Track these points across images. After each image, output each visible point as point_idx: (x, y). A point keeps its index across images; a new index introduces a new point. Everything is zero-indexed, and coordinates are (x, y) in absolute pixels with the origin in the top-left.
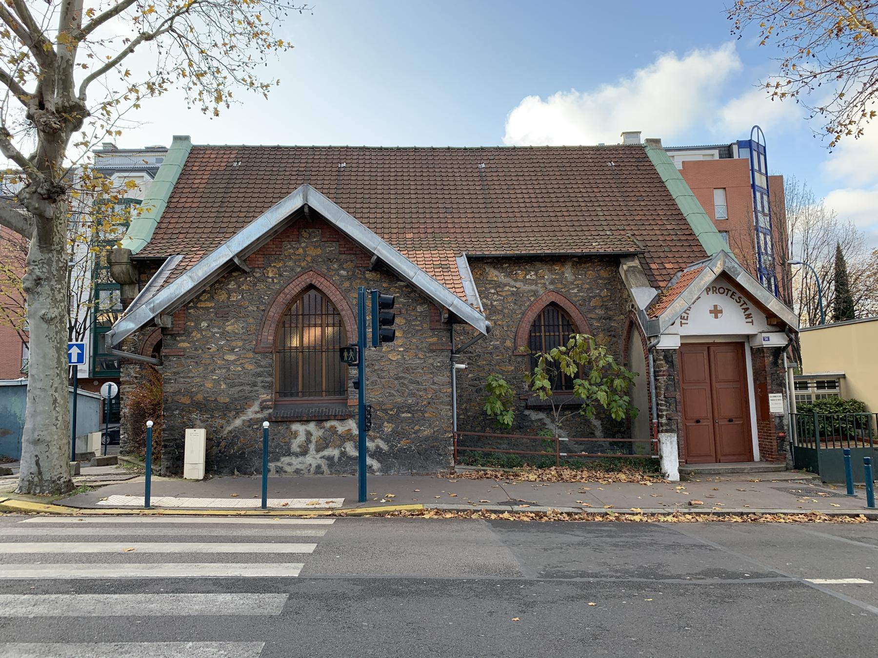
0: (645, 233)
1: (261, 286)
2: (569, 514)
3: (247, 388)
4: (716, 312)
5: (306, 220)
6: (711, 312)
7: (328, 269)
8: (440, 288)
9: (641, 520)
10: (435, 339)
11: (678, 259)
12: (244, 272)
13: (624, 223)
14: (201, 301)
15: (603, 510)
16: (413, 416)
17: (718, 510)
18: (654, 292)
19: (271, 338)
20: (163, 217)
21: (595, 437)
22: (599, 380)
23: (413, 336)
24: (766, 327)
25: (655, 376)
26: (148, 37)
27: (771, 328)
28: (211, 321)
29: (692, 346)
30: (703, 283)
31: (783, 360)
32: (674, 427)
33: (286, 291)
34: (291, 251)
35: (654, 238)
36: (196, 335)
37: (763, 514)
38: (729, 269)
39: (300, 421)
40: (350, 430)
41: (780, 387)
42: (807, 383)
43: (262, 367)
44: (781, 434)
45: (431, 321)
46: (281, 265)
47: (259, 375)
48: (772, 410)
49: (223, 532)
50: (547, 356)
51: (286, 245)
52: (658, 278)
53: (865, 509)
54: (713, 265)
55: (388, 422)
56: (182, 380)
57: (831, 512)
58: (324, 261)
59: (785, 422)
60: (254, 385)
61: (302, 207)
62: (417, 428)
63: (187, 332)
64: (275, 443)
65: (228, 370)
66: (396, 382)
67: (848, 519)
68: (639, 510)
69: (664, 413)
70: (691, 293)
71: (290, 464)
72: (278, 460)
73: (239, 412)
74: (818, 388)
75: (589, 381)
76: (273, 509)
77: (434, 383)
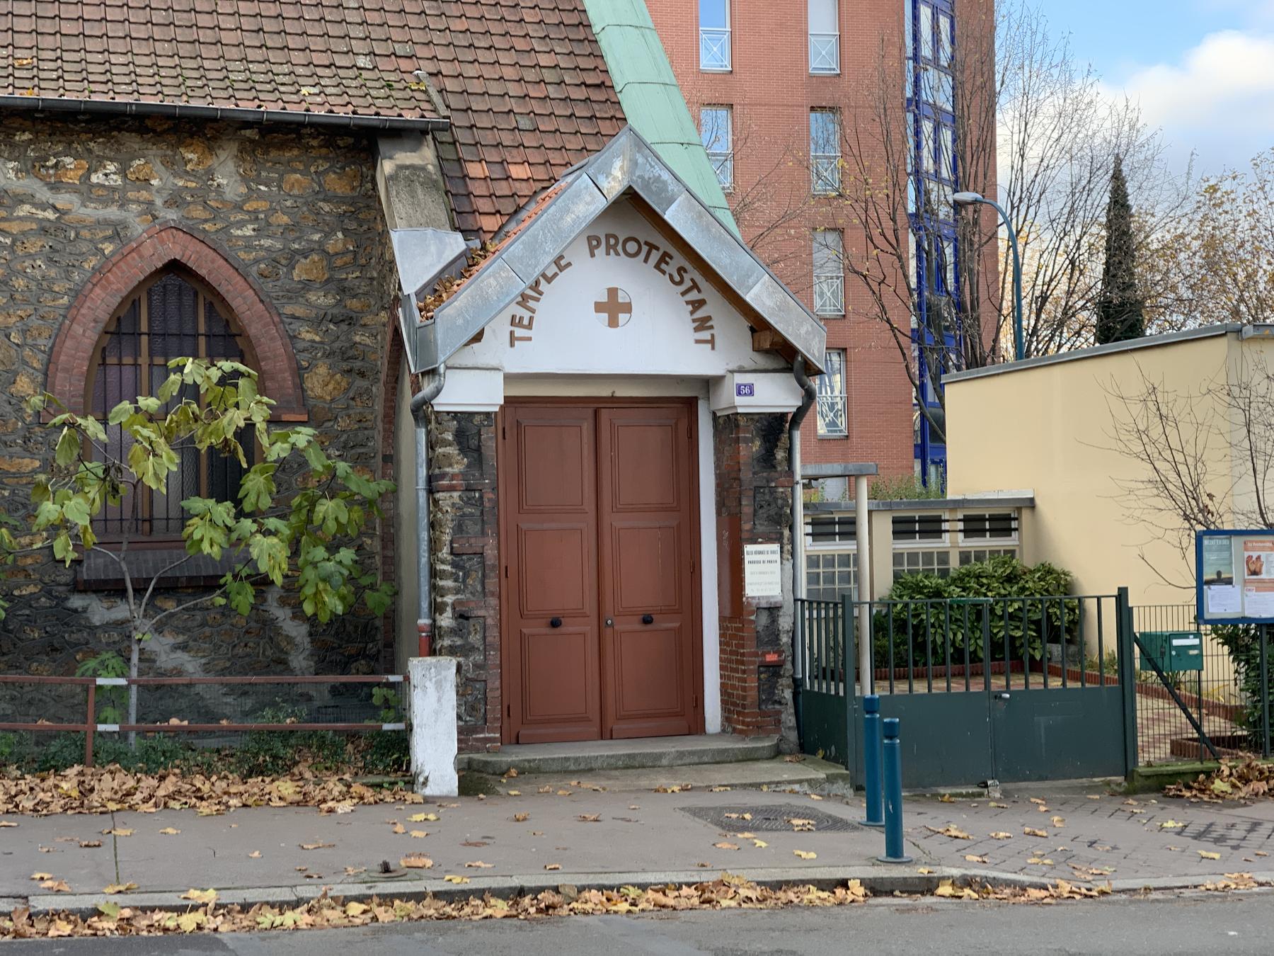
0: (470, 71)
4: (613, 308)
6: (599, 307)
9: (199, 927)
13: (417, 36)
15: (86, 902)
17: (458, 882)
18: (456, 244)
21: (289, 670)
22: (266, 502)
24: (748, 356)
25: (431, 491)
27: (761, 361)
29: (534, 410)
30: (569, 219)
31: (790, 451)
32: (475, 639)
35: (495, 88)
37: (581, 889)
38: (646, 184)
41: (777, 526)
42: (939, 520)
44: (771, 658)
50: (91, 426)
59: (785, 623)
67: (814, 894)
68: (211, 896)
69: (449, 599)
74: (968, 533)
75: (238, 503)
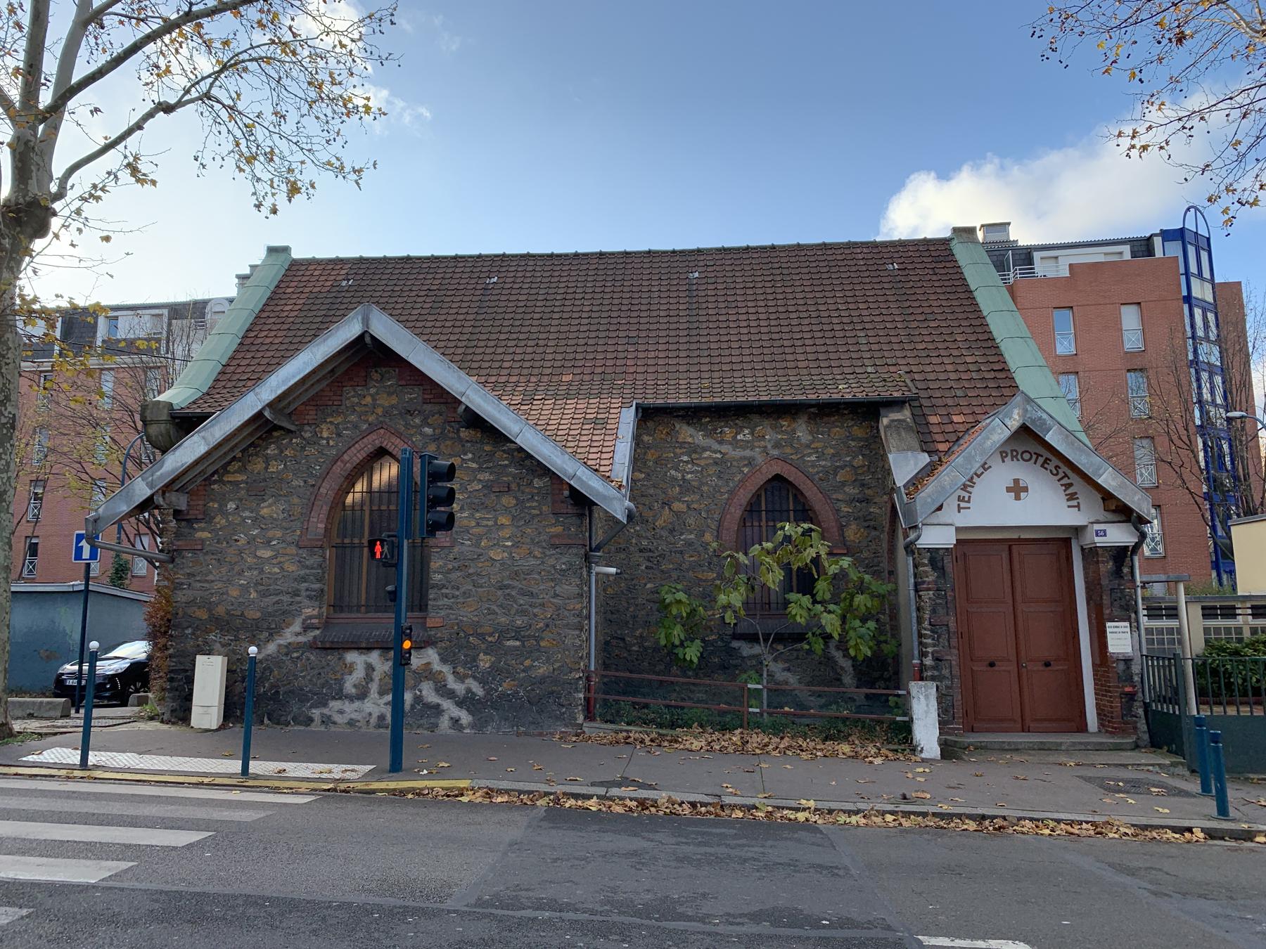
0: (928, 369)
1: (310, 450)
2: (693, 805)
3: (286, 598)
4: (1017, 490)
5: (368, 356)
6: (1009, 490)
7: (407, 425)
8: (558, 452)
9: (807, 820)
10: (559, 529)
11: (975, 409)
12: (290, 431)
13: (899, 354)
14: (229, 472)
15: (750, 801)
16: (524, 646)
17: (946, 808)
18: (925, 459)
19: (322, 526)
20: (232, 358)
21: (841, 684)
22: (828, 596)
23: (527, 523)
24: (1102, 515)
25: (917, 591)
26: (168, 108)
27: (1110, 516)
28: (241, 500)
29: (973, 546)
30: (989, 443)
31: (1132, 568)
32: (946, 672)
33: (346, 457)
34: (356, 400)
35: (942, 376)
36: (220, 521)
37: (1020, 819)
38: (1033, 421)
39: (358, 649)
40: (429, 663)
41: (1127, 612)
42: (1234, 608)
43: (307, 567)
44: (1128, 689)
45: (554, 502)
46: (340, 419)
47: (304, 579)
48: (1111, 649)
49: (116, 809)
50: (741, 556)
51: (349, 392)
52: (938, 437)
53: (1211, 818)
54: (1006, 416)
55: (486, 654)
56: (199, 585)
57: (1144, 821)
58: (400, 414)
59: (1136, 669)
60: (296, 593)
61: (361, 338)
62: (527, 663)
63: (207, 517)
64: (322, 681)
65: (262, 571)
66: (499, 593)
67: (1170, 835)
68: (812, 804)
69: (930, 650)
70: (969, 460)
71: (341, 712)
72: (325, 705)
73: (274, 632)
74: (1254, 616)
75: (813, 596)
76: (257, 777)
77: (556, 596)
